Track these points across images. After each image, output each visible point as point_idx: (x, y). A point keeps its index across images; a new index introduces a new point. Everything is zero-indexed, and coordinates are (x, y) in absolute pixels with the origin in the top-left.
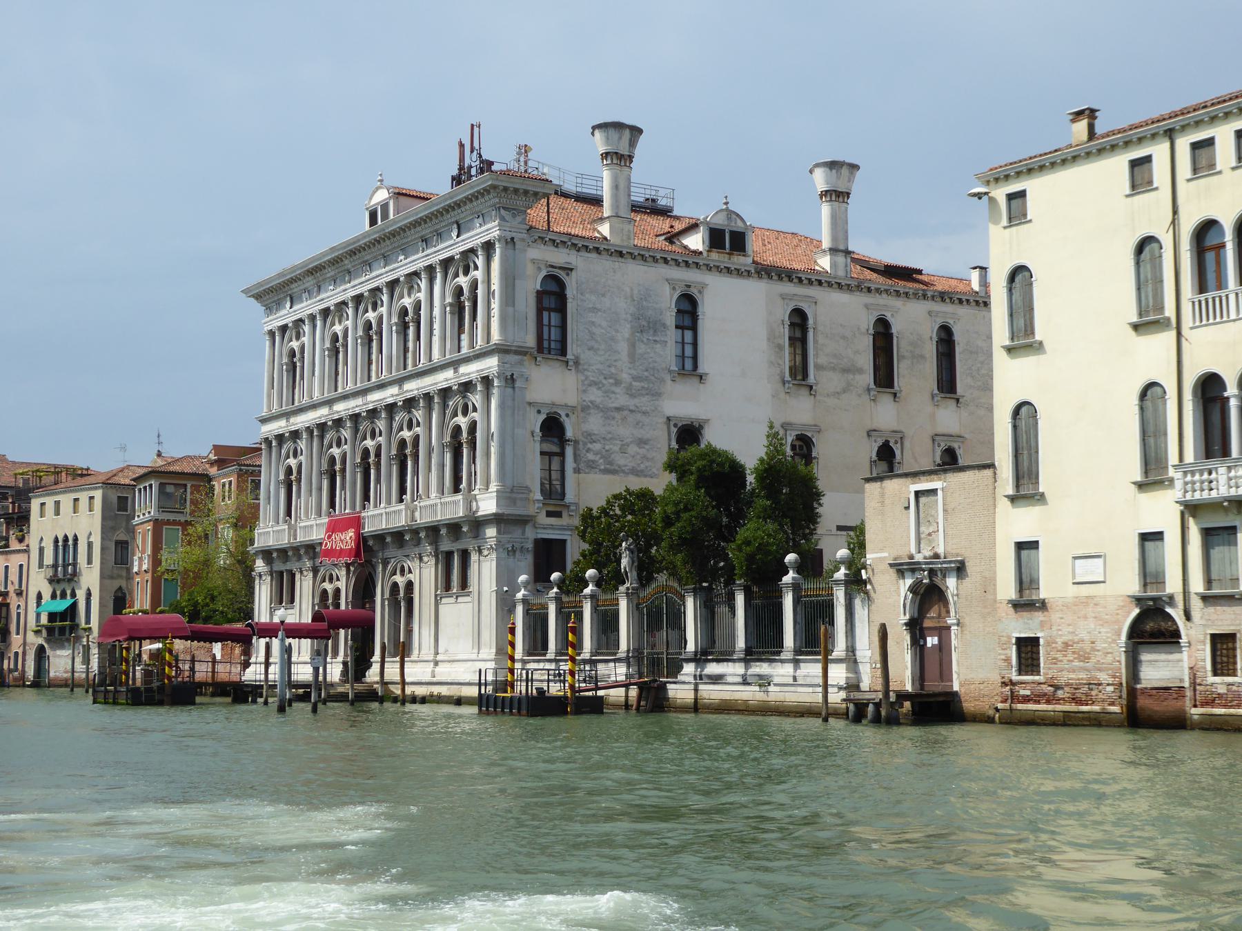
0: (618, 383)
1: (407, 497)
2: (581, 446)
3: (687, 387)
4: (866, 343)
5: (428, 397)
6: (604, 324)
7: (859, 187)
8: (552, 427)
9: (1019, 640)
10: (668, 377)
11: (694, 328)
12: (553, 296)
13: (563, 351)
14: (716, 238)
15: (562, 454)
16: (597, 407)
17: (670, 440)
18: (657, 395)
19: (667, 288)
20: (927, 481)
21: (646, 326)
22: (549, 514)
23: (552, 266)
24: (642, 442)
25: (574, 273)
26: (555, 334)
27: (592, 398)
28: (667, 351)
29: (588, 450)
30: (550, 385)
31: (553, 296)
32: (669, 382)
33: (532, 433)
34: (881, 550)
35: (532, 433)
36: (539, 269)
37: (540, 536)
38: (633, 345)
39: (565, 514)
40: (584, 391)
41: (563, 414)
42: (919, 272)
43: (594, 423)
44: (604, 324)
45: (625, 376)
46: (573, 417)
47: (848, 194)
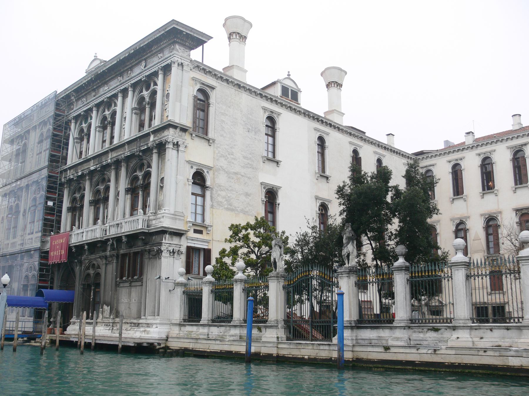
1: (100, 221)
2: (214, 192)
3: (271, 166)
11: (273, 136)
14: (285, 90)
15: (203, 196)
19: (262, 111)
22: (196, 231)
23: (203, 84)
24: (247, 195)
25: (214, 91)
32: (262, 163)
35: (188, 179)
37: (189, 245)
39: (204, 232)
41: (205, 171)
42: (365, 133)
46: (211, 172)
47: (342, 85)
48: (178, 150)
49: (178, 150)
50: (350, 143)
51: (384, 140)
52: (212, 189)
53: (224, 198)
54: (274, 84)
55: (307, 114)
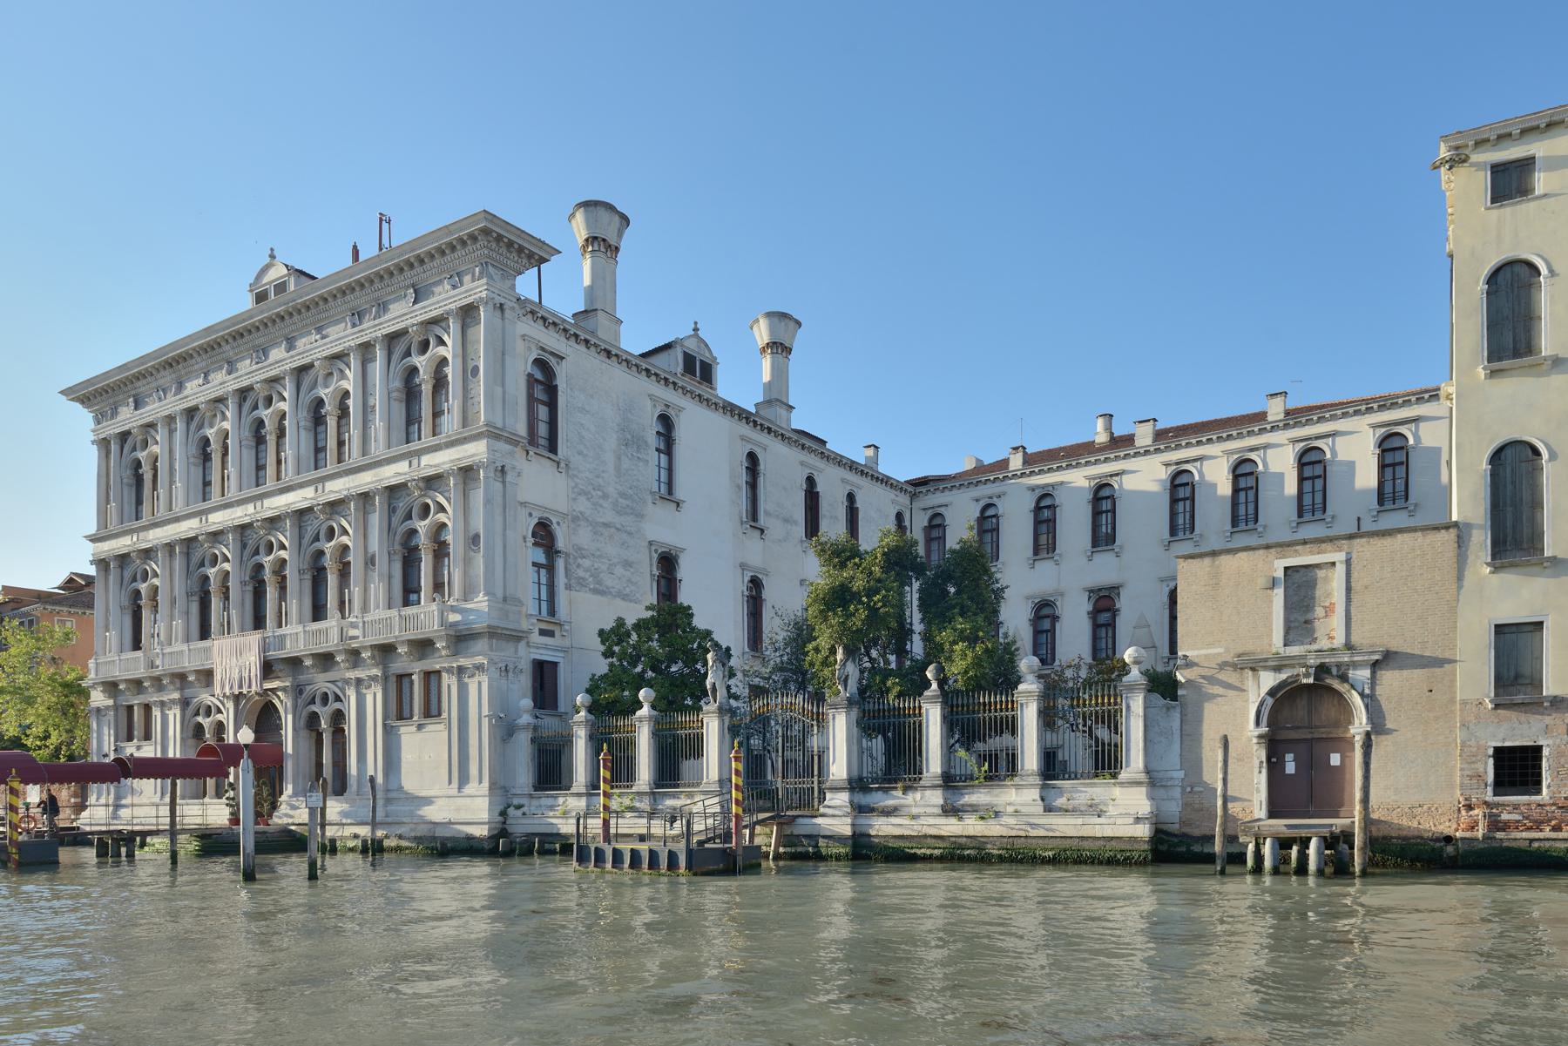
3: (664, 511)
4: (800, 498)
5: (365, 497)
7: (801, 343)
8: (544, 534)
9: (1500, 753)
10: (649, 499)
12: (544, 384)
13: (553, 447)
14: (689, 360)
18: (640, 516)
19: (649, 403)
20: (1312, 553)
21: (632, 441)
26: (543, 430)
28: (649, 468)
30: (540, 486)
31: (544, 384)
33: (525, 538)
34: (1210, 645)
35: (525, 538)
36: (529, 349)
38: (619, 458)
42: (824, 442)
43: (584, 537)
45: (611, 490)
48: (504, 482)
49: (504, 482)
50: (802, 463)
51: (861, 457)
54: (667, 347)
55: (731, 409)
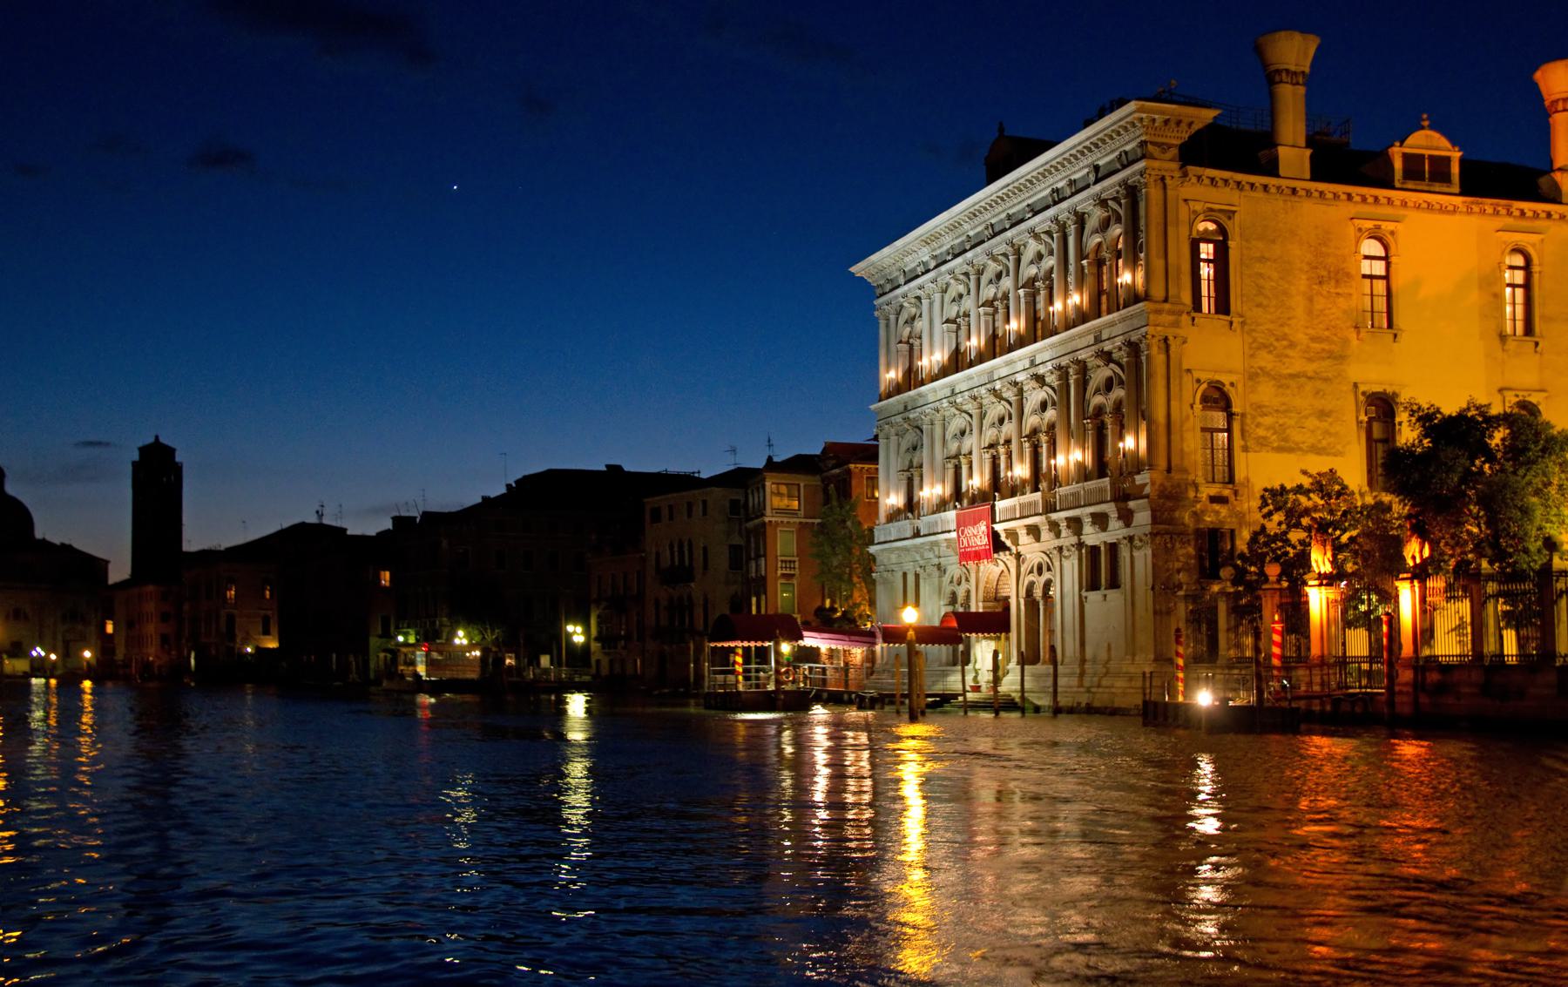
0: (1292, 345)
2: (1248, 421)
6: (1275, 275)
16: (1268, 374)
17: (1358, 411)
18: (1339, 358)
27: (1263, 364)
29: (1258, 425)
38: (1311, 300)
40: (1252, 356)
41: (1227, 383)
44: (1275, 275)
45: (1301, 337)
52: (1243, 415)
53: (1268, 429)
